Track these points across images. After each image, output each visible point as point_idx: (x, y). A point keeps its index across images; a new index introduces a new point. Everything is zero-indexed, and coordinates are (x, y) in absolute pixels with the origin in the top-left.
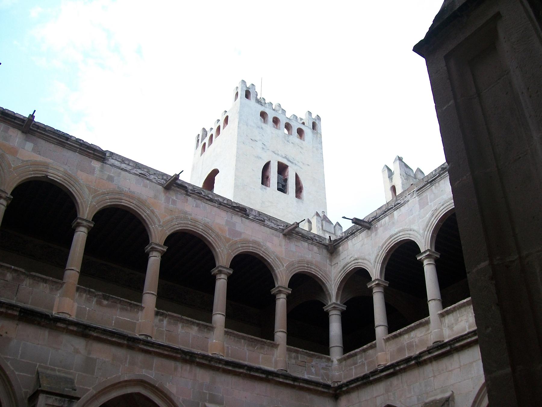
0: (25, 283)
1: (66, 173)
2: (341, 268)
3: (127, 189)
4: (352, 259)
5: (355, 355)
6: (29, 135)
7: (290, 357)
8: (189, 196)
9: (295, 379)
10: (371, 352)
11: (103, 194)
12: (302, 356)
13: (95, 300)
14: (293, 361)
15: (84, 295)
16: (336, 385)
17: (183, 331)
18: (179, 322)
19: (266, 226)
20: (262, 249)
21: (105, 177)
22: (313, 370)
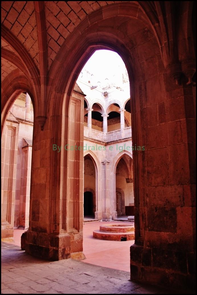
2: (109, 102)
4: (113, 100)
5: (113, 133)
7: (92, 132)
9: (95, 140)
10: (118, 132)
12: (96, 131)
14: (93, 134)
16: (106, 142)
22: (99, 137)
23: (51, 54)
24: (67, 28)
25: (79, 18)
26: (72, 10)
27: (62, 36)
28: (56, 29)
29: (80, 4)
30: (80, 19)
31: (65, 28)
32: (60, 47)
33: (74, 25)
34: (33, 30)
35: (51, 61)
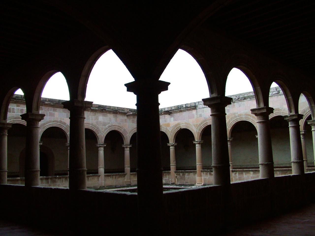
0: (186, 175)
1: (186, 123)
3: (208, 117)
6: (171, 114)
8: (235, 102)
11: (200, 124)
13: (208, 173)
15: (205, 173)
17: (246, 176)
18: (243, 172)
19: (281, 95)
20: (282, 111)
21: (199, 116)
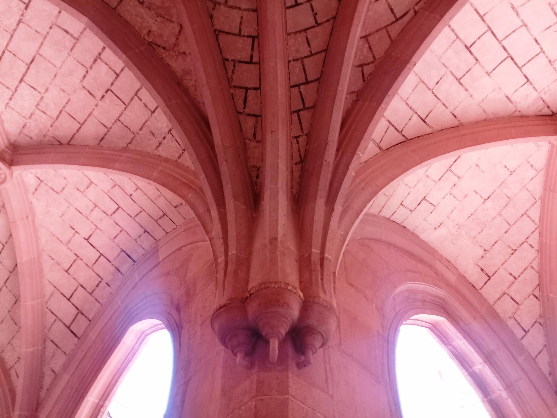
23: (53, 356)
24: (93, 294)
25: (119, 271)
26: (101, 255)
27: (82, 314)
28: (68, 297)
29: (115, 240)
30: (121, 273)
31: (89, 295)
32: (76, 339)
33: (109, 286)
34: (15, 304)
35: (52, 374)
